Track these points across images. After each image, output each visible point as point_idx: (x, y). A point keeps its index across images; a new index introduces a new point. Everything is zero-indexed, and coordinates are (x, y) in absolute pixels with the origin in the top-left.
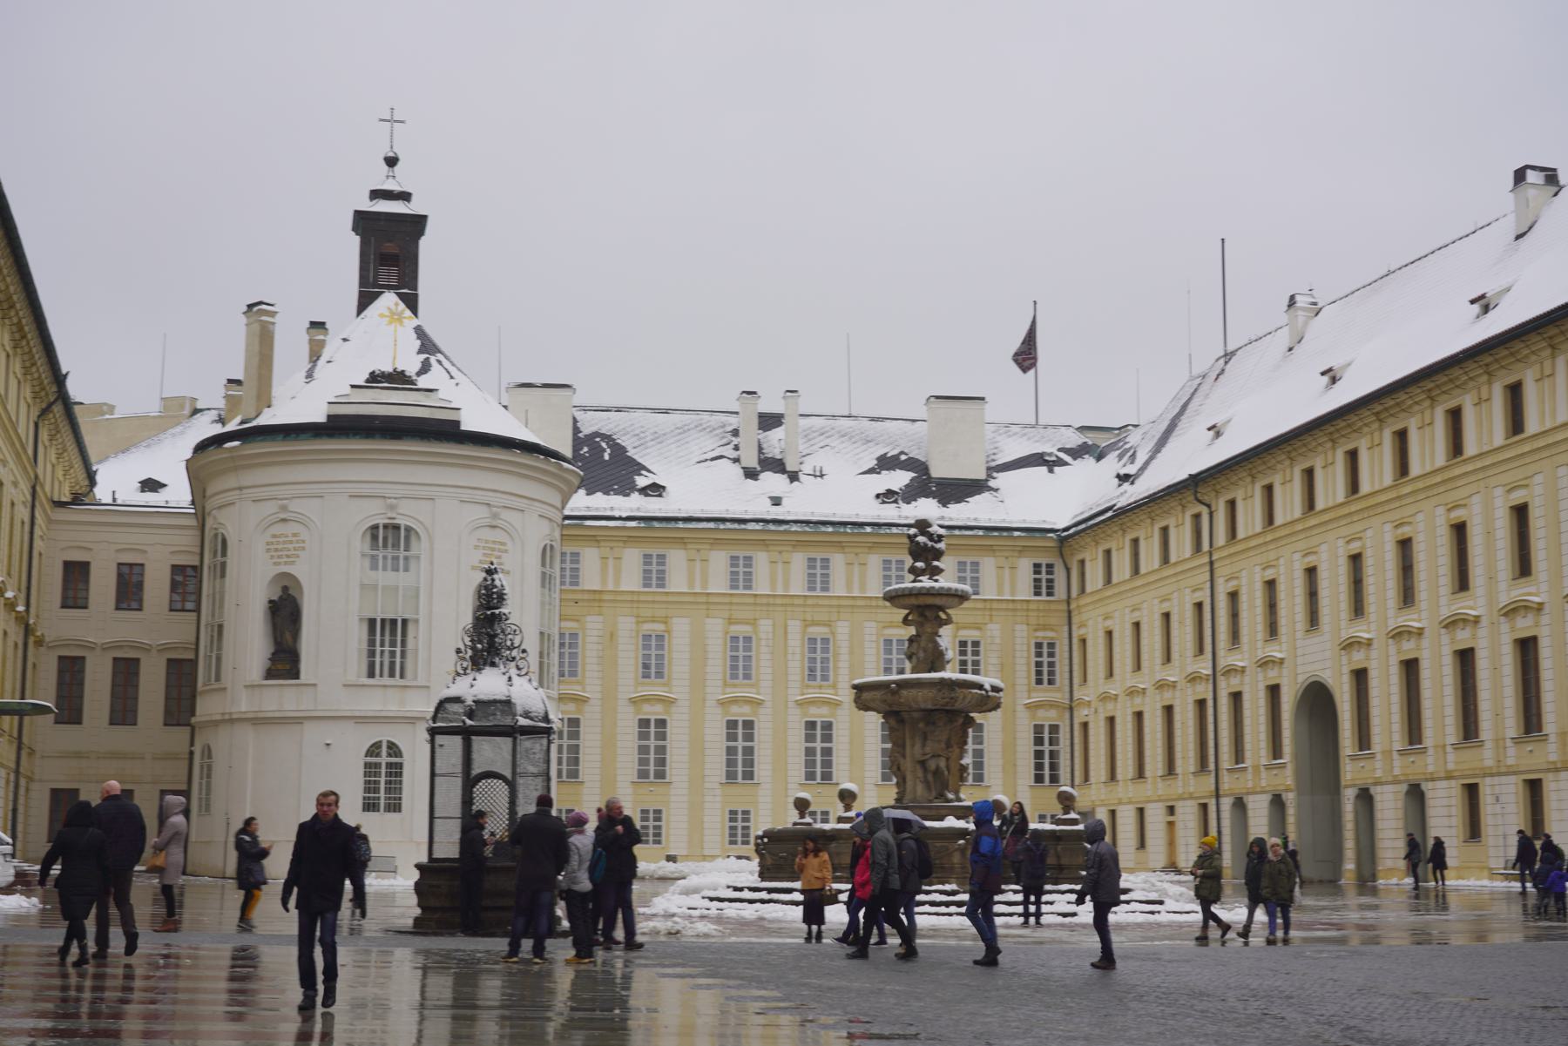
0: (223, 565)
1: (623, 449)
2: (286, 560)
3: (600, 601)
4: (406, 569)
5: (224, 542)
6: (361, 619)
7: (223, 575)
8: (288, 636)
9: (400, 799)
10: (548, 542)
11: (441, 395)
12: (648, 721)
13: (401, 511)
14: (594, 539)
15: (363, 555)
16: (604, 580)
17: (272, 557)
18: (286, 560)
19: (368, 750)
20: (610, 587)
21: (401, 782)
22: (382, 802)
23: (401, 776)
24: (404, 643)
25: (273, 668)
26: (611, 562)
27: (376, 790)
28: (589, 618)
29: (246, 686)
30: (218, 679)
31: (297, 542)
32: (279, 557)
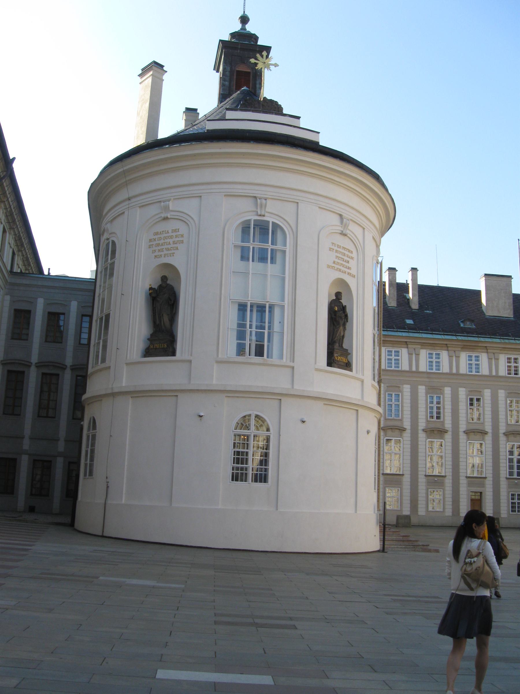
4: (273, 261)
7: (112, 275)
8: (166, 319)
9: (266, 470)
11: (303, 123)
15: (236, 246)
25: (152, 347)
29: (127, 364)
30: (104, 360)
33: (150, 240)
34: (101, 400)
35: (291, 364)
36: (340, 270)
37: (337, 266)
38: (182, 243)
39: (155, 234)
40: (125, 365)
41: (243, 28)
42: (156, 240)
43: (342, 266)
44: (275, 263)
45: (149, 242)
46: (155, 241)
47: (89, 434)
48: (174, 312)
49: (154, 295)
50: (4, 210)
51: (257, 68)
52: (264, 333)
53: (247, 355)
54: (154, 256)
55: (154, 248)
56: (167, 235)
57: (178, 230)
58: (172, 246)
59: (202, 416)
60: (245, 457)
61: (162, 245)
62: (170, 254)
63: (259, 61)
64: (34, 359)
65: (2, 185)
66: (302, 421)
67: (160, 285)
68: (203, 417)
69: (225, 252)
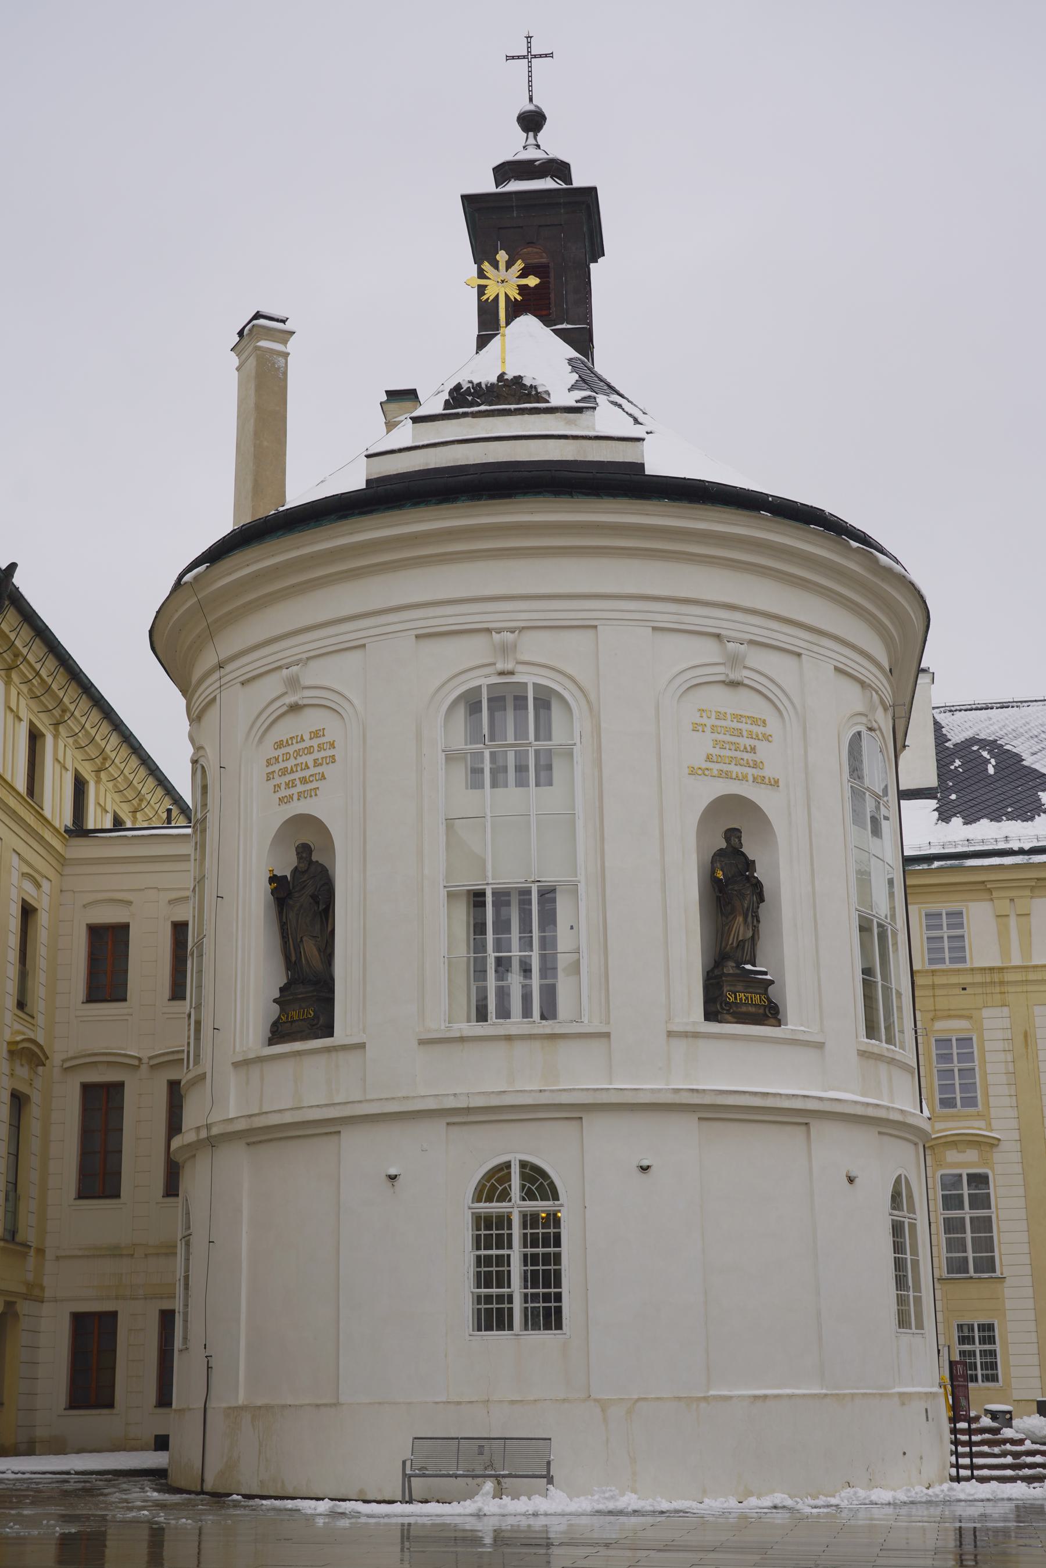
1: (1018, 758)
2: (300, 788)
3: (1002, 983)
6: (451, 895)
8: (310, 948)
9: (558, 1297)
14: (983, 889)
15: (451, 757)
16: (1005, 951)
17: (277, 788)
18: (300, 788)
20: (1016, 961)
21: (558, 1258)
23: (558, 1243)
24: (548, 944)
26: (1013, 921)
27: (503, 1279)
28: (986, 1013)
29: (236, 1065)
31: (320, 748)
32: (291, 784)
34: (194, 1156)
36: (727, 775)
37: (715, 767)
38: (332, 762)
39: (278, 746)
42: (280, 759)
43: (734, 762)
44: (551, 784)
45: (267, 766)
46: (279, 762)
47: (188, 1237)
48: (330, 929)
50: (22, 687)
53: (492, 1017)
54: (278, 800)
55: (277, 780)
56: (302, 745)
57: (322, 731)
58: (313, 771)
59: (396, 1176)
60: (506, 1268)
61: (292, 772)
62: (309, 792)
63: (488, 278)
66: (641, 1167)
67: (296, 868)
68: (397, 1178)
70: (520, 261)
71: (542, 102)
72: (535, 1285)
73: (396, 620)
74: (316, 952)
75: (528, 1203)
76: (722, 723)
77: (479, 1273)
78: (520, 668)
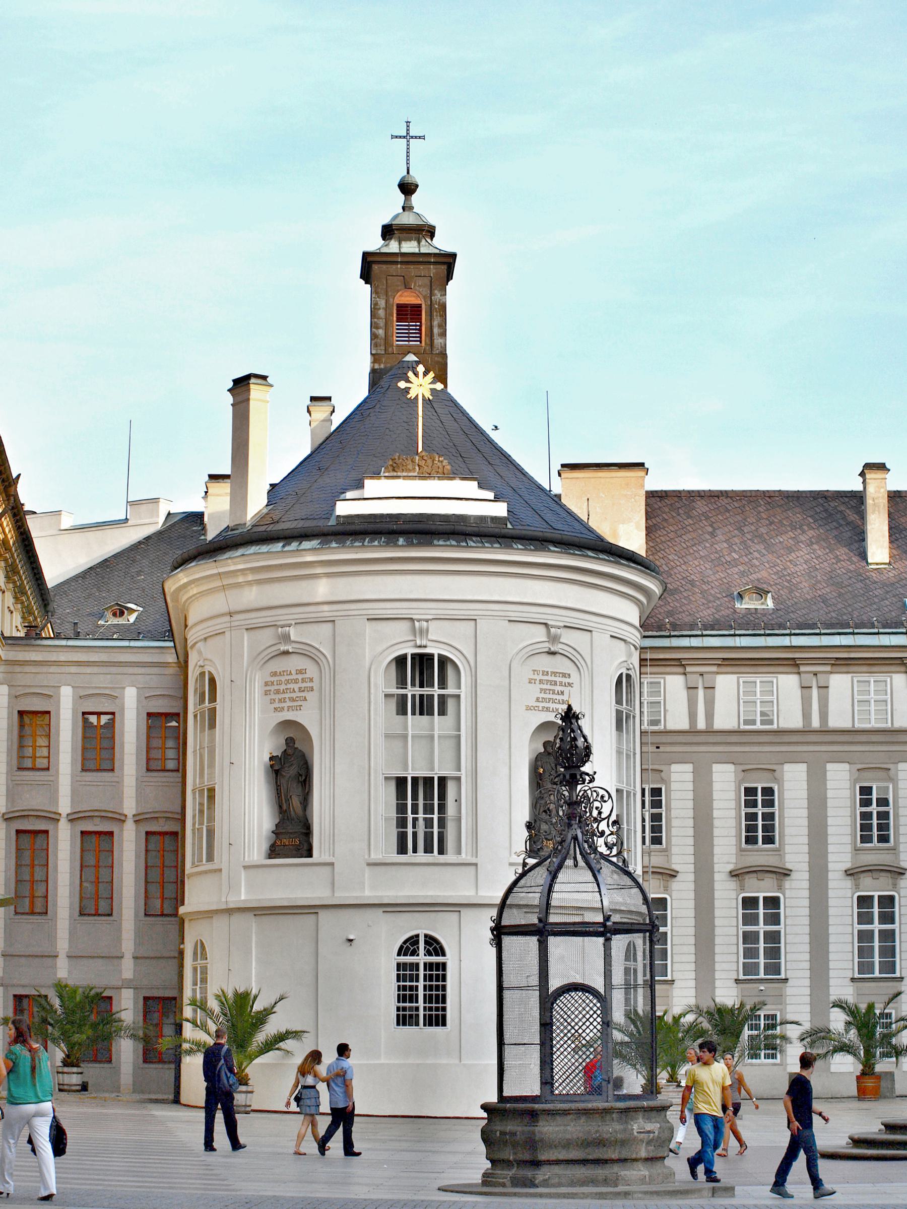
0: (213, 712)
2: (289, 704)
4: (442, 712)
5: (212, 681)
7: (212, 725)
9: (444, 1009)
10: (625, 671)
12: (756, 899)
13: (430, 637)
17: (272, 701)
18: (289, 704)
19: (401, 948)
21: (444, 988)
22: (421, 1013)
23: (444, 978)
24: (442, 808)
27: (413, 998)
29: (245, 867)
30: (210, 858)
31: (303, 680)
33: (265, 682)
35: (474, 861)
37: (541, 705)
40: (242, 869)
41: (407, 208)
42: (275, 683)
49: (276, 768)
51: (409, 396)
52: (433, 818)
55: (273, 697)
60: (414, 993)
61: (284, 692)
64: (64, 807)
65: (1, 525)
69: (372, 704)
70: (432, 372)
71: (416, 176)
72: (431, 1002)
73: (355, 608)
74: (299, 805)
75: (428, 957)
76: (545, 678)
77: (399, 995)
78: (429, 644)
